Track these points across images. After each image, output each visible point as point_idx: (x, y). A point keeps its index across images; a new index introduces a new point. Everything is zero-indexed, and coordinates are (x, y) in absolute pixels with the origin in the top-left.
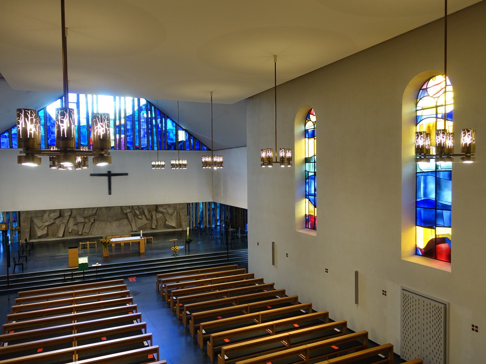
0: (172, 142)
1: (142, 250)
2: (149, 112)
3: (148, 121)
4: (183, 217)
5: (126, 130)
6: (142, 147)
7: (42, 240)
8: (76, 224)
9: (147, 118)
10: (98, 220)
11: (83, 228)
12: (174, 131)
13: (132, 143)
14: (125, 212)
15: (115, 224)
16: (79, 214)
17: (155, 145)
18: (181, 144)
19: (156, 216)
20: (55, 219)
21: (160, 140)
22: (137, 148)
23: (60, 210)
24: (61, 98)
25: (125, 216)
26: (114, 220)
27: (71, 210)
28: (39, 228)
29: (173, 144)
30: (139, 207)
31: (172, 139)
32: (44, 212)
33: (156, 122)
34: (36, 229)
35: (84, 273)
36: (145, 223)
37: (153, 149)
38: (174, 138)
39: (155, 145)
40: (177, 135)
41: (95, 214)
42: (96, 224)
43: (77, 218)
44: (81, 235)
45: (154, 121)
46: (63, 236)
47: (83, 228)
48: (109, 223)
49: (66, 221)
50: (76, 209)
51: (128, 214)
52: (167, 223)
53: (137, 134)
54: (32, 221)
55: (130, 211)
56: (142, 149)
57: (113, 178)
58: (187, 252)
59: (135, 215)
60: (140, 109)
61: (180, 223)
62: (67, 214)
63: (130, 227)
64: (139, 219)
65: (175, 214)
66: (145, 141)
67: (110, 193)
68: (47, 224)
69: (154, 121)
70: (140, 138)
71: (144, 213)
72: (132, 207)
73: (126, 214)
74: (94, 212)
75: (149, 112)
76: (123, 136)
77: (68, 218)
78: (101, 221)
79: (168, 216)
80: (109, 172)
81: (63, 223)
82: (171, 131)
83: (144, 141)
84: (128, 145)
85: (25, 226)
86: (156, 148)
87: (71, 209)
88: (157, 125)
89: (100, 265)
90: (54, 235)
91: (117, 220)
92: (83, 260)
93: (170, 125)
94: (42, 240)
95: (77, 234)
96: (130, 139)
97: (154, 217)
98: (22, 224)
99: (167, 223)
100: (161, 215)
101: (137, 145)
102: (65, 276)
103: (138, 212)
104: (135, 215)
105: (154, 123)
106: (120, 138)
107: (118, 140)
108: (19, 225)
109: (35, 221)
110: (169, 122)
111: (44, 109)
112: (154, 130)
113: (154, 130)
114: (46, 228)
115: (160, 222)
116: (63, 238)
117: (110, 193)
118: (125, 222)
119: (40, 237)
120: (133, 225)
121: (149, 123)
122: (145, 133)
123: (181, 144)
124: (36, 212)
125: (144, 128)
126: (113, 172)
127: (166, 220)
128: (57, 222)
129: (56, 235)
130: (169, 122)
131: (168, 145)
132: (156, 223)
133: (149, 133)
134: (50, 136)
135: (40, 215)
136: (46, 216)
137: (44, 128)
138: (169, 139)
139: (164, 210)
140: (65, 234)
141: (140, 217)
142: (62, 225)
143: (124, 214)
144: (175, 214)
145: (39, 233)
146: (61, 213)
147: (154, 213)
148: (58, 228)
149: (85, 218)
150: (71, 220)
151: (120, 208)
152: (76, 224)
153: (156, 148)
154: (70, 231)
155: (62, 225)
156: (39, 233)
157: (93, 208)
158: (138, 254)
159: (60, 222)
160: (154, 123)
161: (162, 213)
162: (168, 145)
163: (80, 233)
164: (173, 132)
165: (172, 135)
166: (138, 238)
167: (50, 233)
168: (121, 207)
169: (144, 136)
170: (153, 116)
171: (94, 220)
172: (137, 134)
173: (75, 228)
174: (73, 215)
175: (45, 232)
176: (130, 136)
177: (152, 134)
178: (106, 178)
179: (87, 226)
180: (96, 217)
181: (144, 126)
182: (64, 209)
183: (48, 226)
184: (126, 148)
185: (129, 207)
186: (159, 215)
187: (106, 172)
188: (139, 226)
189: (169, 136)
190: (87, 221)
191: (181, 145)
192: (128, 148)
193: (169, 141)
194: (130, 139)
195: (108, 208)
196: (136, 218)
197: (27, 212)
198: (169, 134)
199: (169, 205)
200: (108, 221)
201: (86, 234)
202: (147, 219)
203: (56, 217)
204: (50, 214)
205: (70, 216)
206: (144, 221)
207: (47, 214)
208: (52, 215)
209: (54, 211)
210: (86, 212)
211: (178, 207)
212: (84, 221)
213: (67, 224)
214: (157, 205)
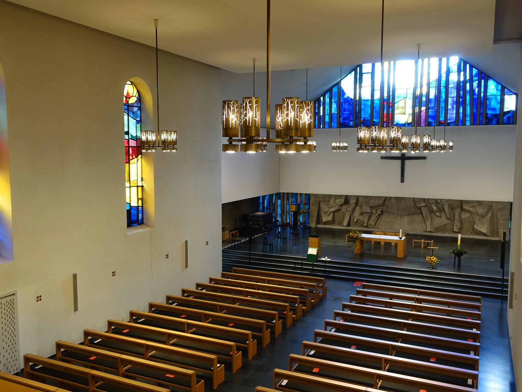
0: (493, 113)
1: (400, 254)
2: (462, 73)
3: (460, 86)
4: (501, 222)
5: (428, 100)
6: (448, 122)
7: (328, 226)
8: (362, 214)
9: (459, 82)
10: (387, 212)
11: (369, 219)
12: (499, 97)
13: (436, 117)
14: (418, 206)
15: (406, 219)
16: (366, 203)
17: (468, 118)
18: (509, 115)
19: (460, 216)
20: (342, 205)
21: (475, 111)
22: (440, 124)
23: (346, 196)
24: (355, 69)
25: (419, 211)
26: (405, 215)
27: (358, 198)
28: (325, 213)
29: (495, 116)
30: (436, 202)
31: (494, 109)
32: (330, 196)
33: (471, 86)
34: (322, 214)
35: (313, 265)
36: (445, 223)
37: (463, 123)
38: (498, 106)
39: (468, 118)
40: (502, 102)
41: (383, 205)
42: (384, 217)
43: (363, 206)
44: (367, 227)
45: (468, 85)
46: (349, 225)
47: (369, 219)
48: (399, 218)
49: (350, 209)
50: (363, 196)
51: (422, 209)
52: (475, 227)
53: (442, 105)
54: (319, 205)
55: (424, 205)
56: (449, 124)
57: (407, 162)
58: (457, 268)
59: (432, 212)
60: (448, 72)
61: (497, 229)
62: (353, 201)
63: (424, 225)
64: (437, 216)
65: (489, 216)
66: (452, 114)
67: (402, 181)
68: (332, 210)
69: (468, 85)
70: (446, 110)
71: (444, 210)
72: (428, 199)
73: (420, 208)
74: (381, 202)
75: (462, 73)
76: (423, 108)
77: (353, 205)
78: (390, 213)
79: (478, 217)
81: (348, 211)
82: (493, 97)
83: (452, 115)
84: (430, 120)
85: (314, 209)
86: (468, 123)
87: (357, 196)
88: (472, 90)
89: (328, 260)
90: (341, 223)
91: (409, 215)
92: (312, 251)
93: (492, 88)
94: (328, 226)
95: (362, 226)
96: (433, 112)
97: (456, 217)
98: (311, 207)
99: (475, 227)
100: (468, 215)
101: (442, 119)
102: (295, 263)
103: (435, 208)
104: (432, 212)
105: (468, 88)
106: (420, 111)
108: (309, 208)
109: (322, 205)
110: (492, 85)
111: (338, 84)
112: (468, 98)
113: (468, 98)
114: (332, 214)
115: (466, 225)
116: (348, 228)
117: (402, 181)
118: (419, 218)
119: (326, 223)
120: (428, 223)
121: (461, 88)
122: (453, 103)
123: (509, 115)
124: (324, 196)
125: (452, 96)
127: (475, 222)
128: (344, 208)
129: (342, 223)
130: (492, 85)
131: (487, 117)
132: (458, 224)
133: (460, 102)
134: (342, 114)
135: (327, 200)
136: (332, 201)
137: (337, 105)
138: (489, 109)
139: (471, 209)
140: (351, 223)
141: (438, 214)
142: (347, 213)
143: (418, 208)
144: (489, 216)
145: (325, 219)
146: (347, 199)
147: (457, 212)
148: (344, 217)
149: (372, 208)
150: (358, 208)
152: (362, 214)
153: (468, 123)
154: (355, 221)
155: (347, 213)
156: (325, 219)
157: (380, 198)
158: (395, 258)
159: (346, 209)
160: (468, 88)
161: (469, 212)
162: (487, 117)
163: (365, 225)
164: (496, 99)
165: (494, 104)
166: (396, 238)
167: (337, 220)
168: (414, 198)
169: (453, 107)
170: (468, 78)
171: (382, 212)
172: (442, 105)
173: (361, 218)
174: (360, 203)
175: (330, 218)
176: (432, 108)
177: (464, 104)
178: (399, 162)
179: (374, 217)
180: (384, 208)
181: (453, 94)
183: (334, 212)
184: (427, 123)
185: (424, 200)
186: (465, 215)
188: (436, 226)
189: (490, 104)
190: (374, 211)
191: (509, 118)
192: (429, 124)
193: (489, 112)
194: (433, 112)
195: (399, 199)
196: (433, 214)
197: (316, 196)
198: (490, 102)
199: (480, 203)
201: (371, 226)
202: (448, 219)
203: (341, 203)
204: (335, 199)
205: (357, 204)
206: (443, 221)
207: (333, 199)
208: (337, 201)
209: (340, 196)
210: (372, 201)
211: (494, 207)
212: (369, 211)
213: (353, 213)
214: (462, 201)
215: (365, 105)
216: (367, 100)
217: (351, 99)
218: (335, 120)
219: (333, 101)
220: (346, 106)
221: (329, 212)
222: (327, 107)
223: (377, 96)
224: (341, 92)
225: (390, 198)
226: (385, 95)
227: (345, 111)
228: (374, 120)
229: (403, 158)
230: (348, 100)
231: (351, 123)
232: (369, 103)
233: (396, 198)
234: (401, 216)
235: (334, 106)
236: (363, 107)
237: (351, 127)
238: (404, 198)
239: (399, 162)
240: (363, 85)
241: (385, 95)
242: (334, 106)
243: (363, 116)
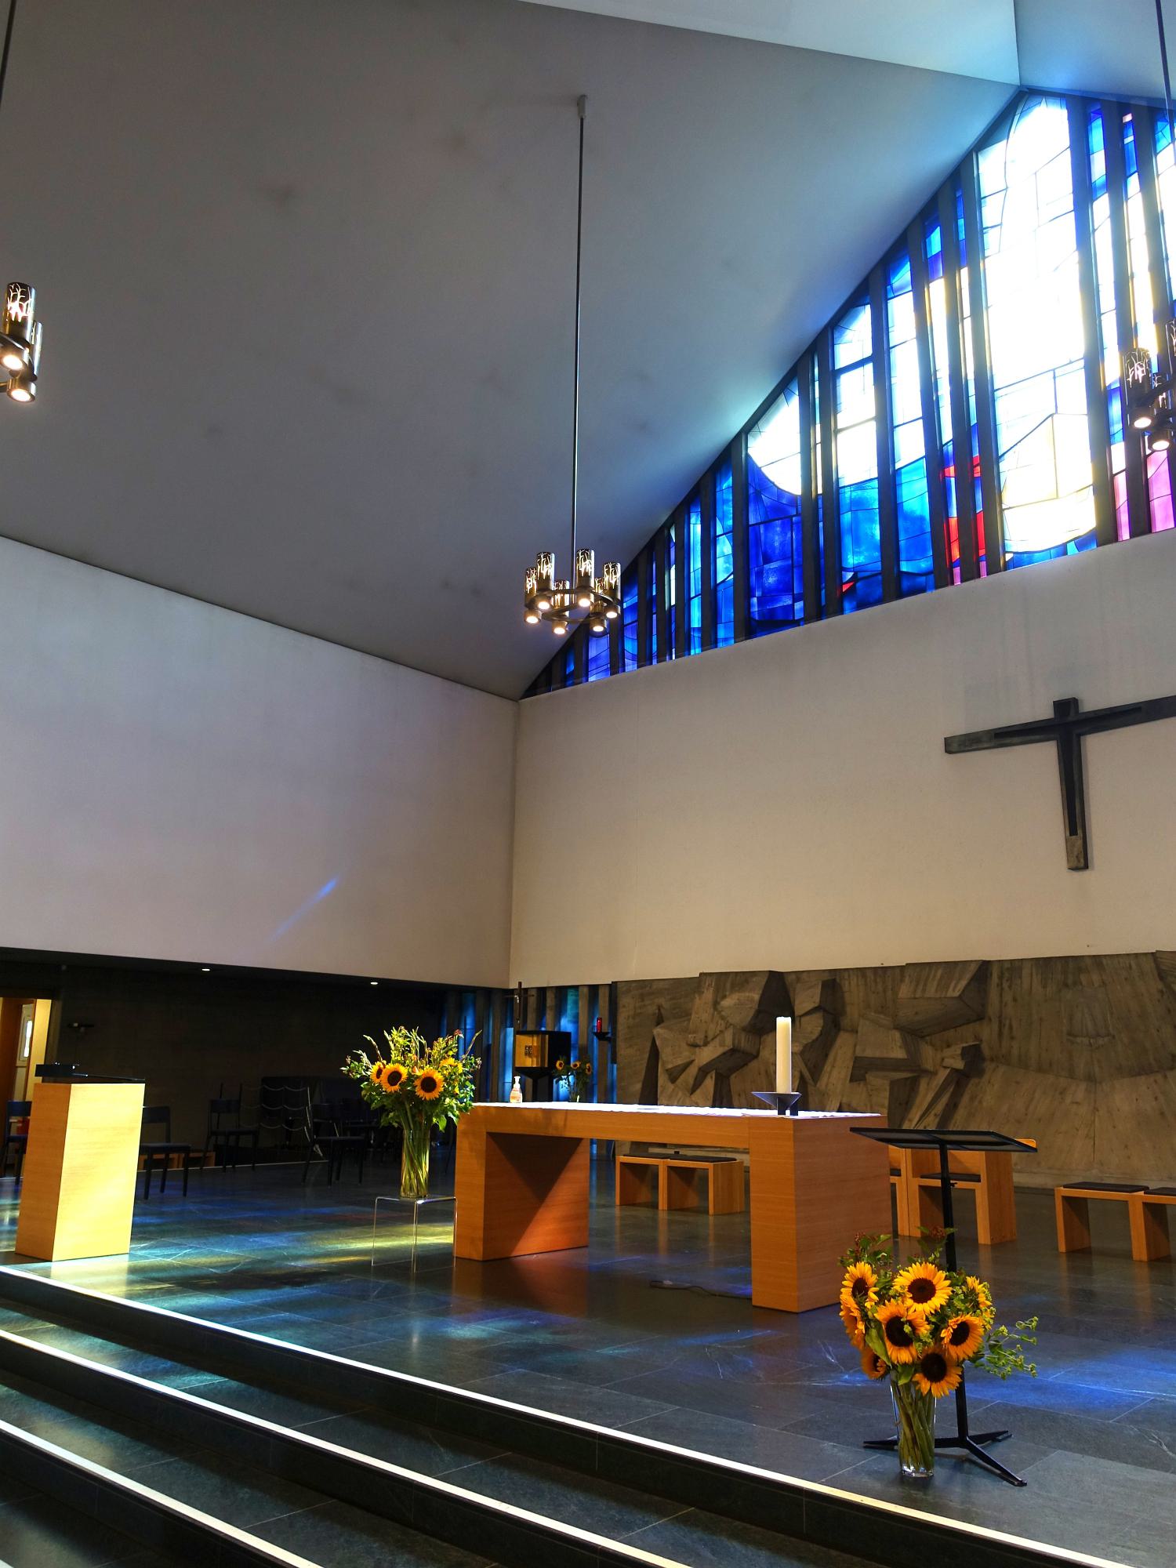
48: (1079, 1091)
50: (862, 971)
68: (707, 1055)
80: (1066, 707)
91: (1142, 1070)
107: (1121, 482)
117: (1081, 860)
126: (1092, 702)
149: (913, 1034)
151: (1149, 966)
168: (1154, 956)
180: (987, 1033)
182: (798, 974)
187: (1045, 712)
190: (928, 1055)
195: (1065, 972)
197: (644, 988)
200: (1072, 1075)
207: (708, 995)
209: (739, 980)
210: (904, 991)
212: (899, 1054)
215: (858, 505)
216: (860, 486)
217: (793, 500)
218: (728, 613)
219: (719, 531)
220: (776, 538)
221: (693, 1071)
222: (696, 563)
223: (910, 446)
224: (752, 485)
225: (1013, 968)
226: (947, 434)
227: (767, 560)
228: (905, 567)
229: (1068, 727)
230: (781, 508)
231: (799, 605)
232: (872, 495)
233: (1045, 964)
234: (1090, 1079)
235: (725, 547)
236: (847, 518)
237: (797, 623)
238: (1097, 960)
239: (1045, 755)
240: (842, 419)
241: (947, 434)
242: (725, 547)
243: (851, 560)
